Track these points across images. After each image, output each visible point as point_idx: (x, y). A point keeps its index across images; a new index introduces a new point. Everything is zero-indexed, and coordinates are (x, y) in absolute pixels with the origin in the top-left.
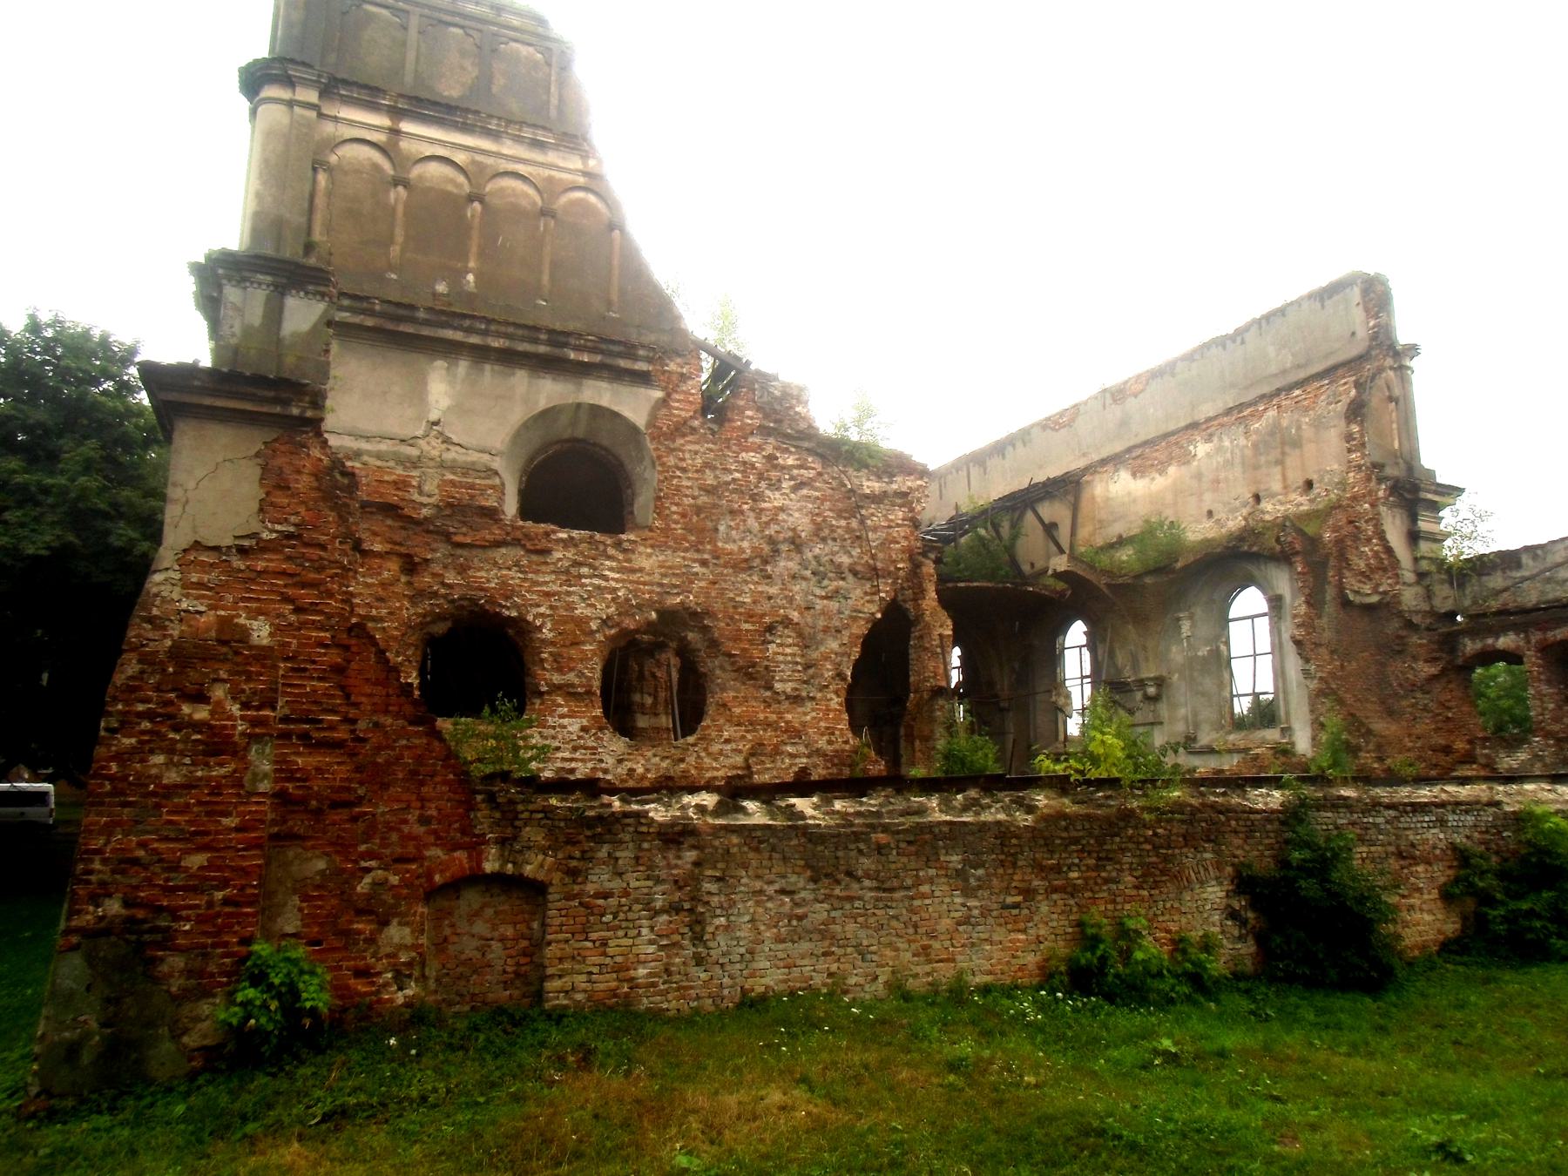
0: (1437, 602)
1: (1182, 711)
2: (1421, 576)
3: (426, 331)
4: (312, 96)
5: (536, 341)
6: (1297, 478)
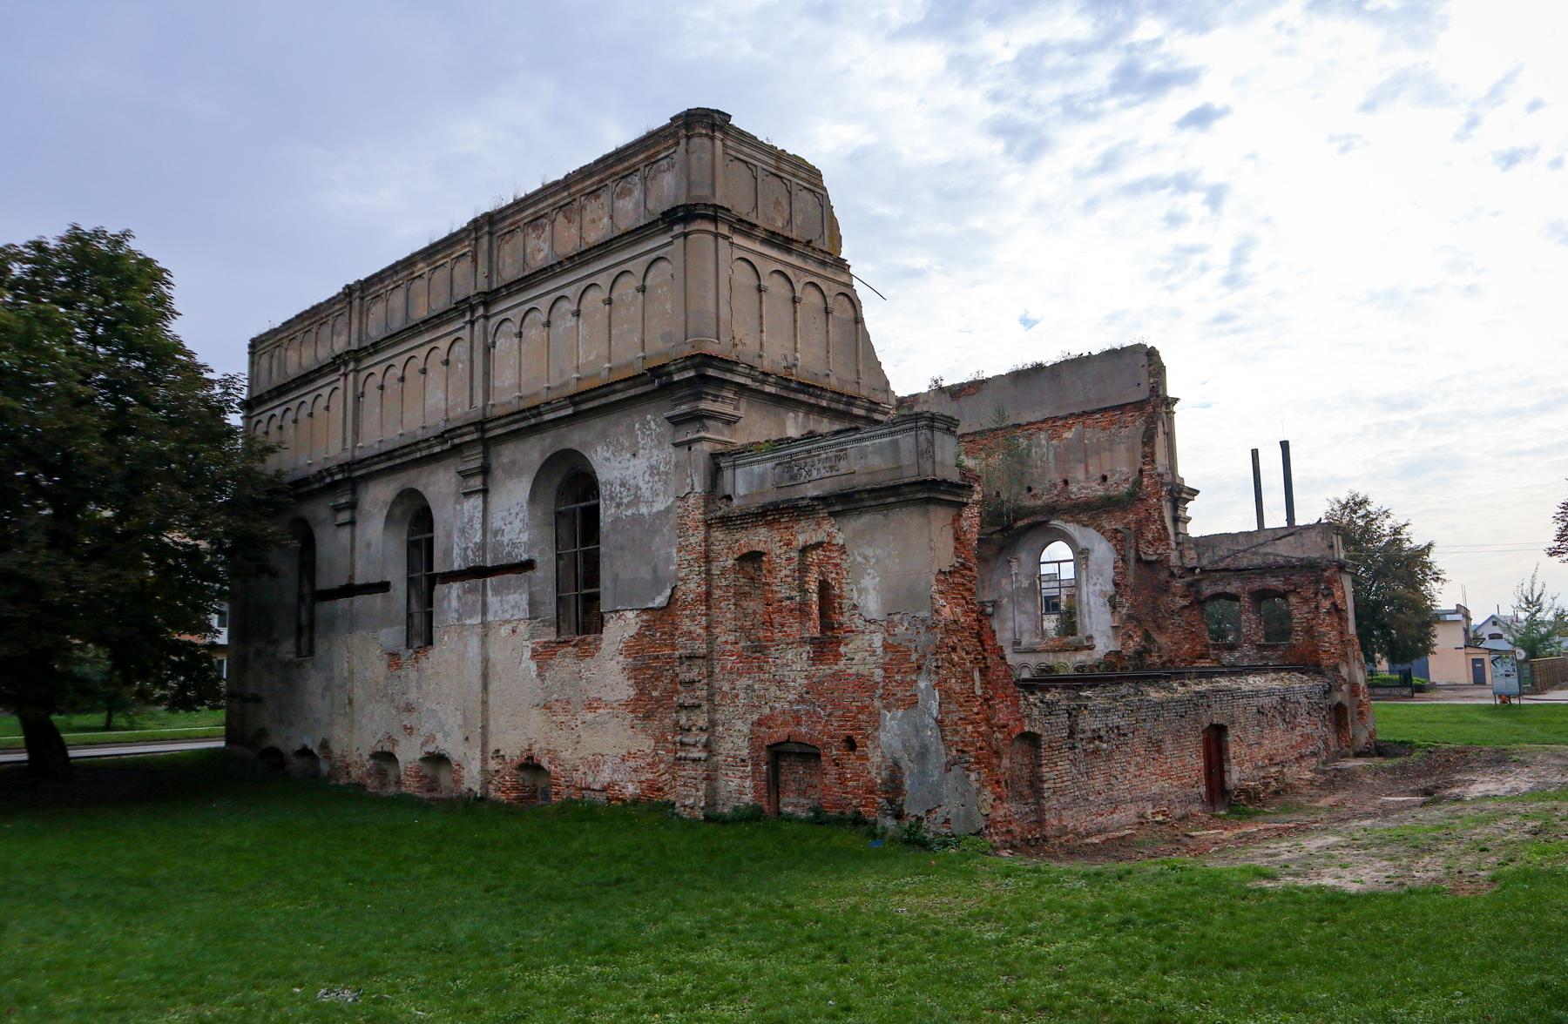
0: (1186, 561)
1: (1010, 624)
2: (1178, 544)
3: (792, 396)
4: (723, 229)
5: (839, 402)
6: (1095, 472)
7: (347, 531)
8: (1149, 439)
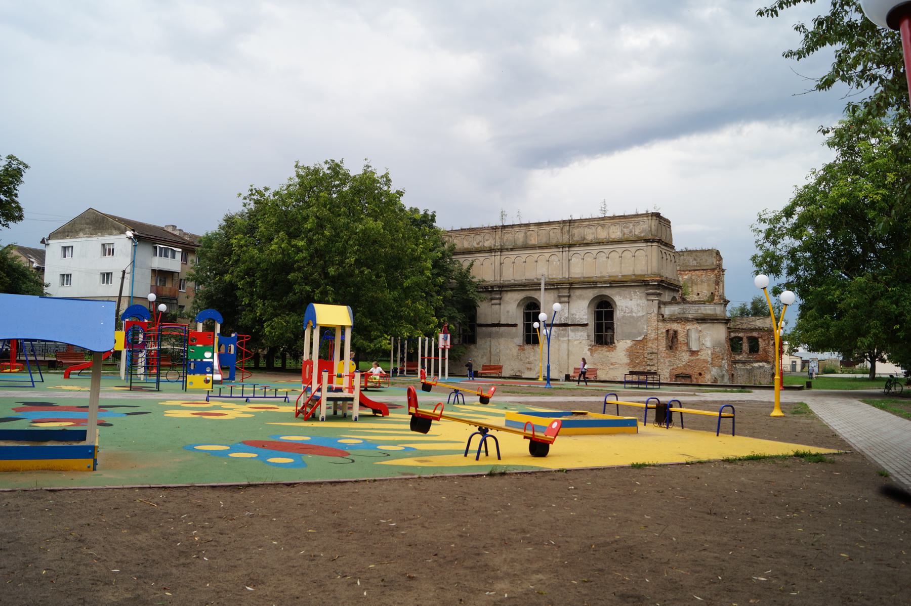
7: (497, 306)
8: (717, 283)
